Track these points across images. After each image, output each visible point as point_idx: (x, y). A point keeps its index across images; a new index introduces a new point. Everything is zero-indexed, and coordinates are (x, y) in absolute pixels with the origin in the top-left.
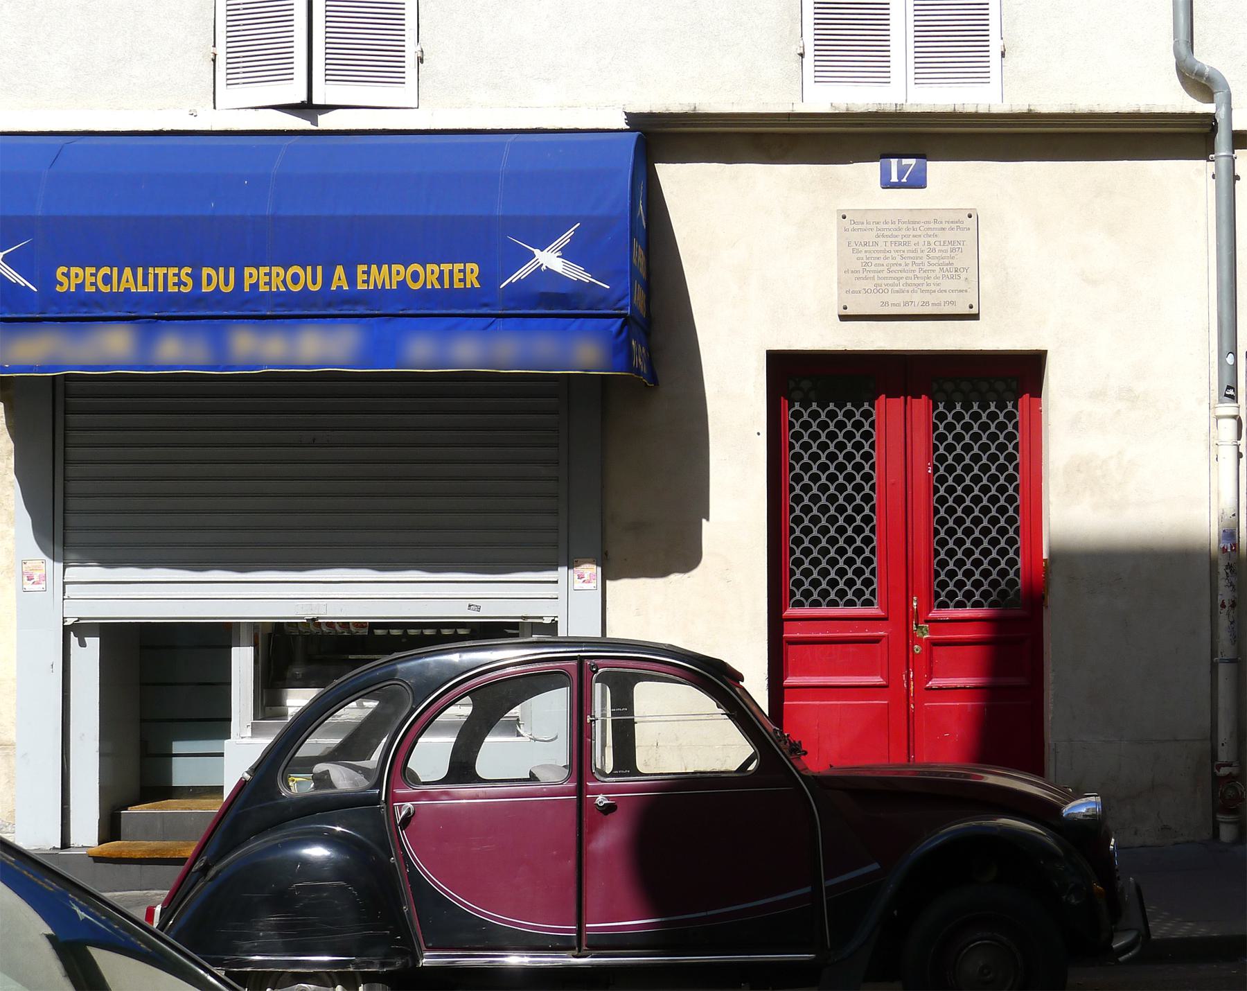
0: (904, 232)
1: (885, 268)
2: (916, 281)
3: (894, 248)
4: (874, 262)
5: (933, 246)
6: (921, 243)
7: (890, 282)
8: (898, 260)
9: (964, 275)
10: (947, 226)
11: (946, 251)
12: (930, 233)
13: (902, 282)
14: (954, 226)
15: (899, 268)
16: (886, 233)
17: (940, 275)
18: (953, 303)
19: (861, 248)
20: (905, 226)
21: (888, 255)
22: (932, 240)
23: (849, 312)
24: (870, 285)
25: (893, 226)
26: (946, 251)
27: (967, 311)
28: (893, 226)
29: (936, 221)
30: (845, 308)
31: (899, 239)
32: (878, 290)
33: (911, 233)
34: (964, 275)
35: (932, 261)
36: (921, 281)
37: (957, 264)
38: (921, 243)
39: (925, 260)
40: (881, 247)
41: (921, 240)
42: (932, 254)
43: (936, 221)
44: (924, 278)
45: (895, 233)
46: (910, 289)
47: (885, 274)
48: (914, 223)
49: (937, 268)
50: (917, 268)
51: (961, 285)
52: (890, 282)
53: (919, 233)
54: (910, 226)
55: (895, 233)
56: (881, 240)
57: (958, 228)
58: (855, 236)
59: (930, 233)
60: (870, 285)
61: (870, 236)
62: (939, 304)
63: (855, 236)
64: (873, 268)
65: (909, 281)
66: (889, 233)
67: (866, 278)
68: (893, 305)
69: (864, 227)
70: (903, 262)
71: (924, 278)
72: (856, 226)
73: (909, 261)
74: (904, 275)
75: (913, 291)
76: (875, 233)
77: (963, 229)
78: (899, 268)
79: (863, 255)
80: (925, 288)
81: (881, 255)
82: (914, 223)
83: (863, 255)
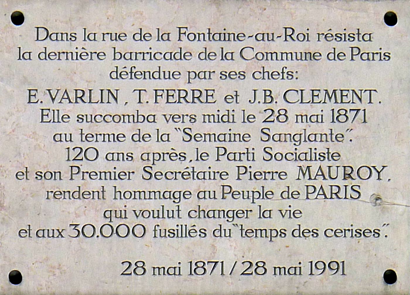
0: (194, 64)
1: (138, 165)
2: (230, 204)
3: (164, 108)
4: (104, 148)
5: (281, 104)
6: (245, 96)
7: (153, 205)
8: (177, 142)
9: (369, 188)
10: (323, 47)
11: (319, 119)
12: (274, 66)
13: (186, 205)
14: (344, 46)
15: (177, 166)
16: (141, 65)
17: (300, 186)
19: (66, 108)
20: (197, 47)
21: (146, 128)
22: (278, 87)
24: (91, 214)
25: (164, 47)
26: (319, 119)
28: (164, 47)
29: (289, 34)
31: (181, 84)
32: (114, 227)
33: (217, 65)
34: (369, 188)
35: (277, 148)
36: (240, 204)
37: (352, 155)
38: (245, 96)
39: (256, 143)
40: (128, 104)
41: (245, 87)
42: (276, 128)
43: (289, 34)
44: (252, 196)
45: (169, 66)
46: (211, 225)
47: (136, 183)
48: (225, 37)
49: (292, 168)
50: (231, 167)
51: (364, 215)
52: (153, 205)
53: (238, 65)
54: (215, 46)
55: (169, 66)
56: (126, 87)
57: (357, 53)
58: (51, 74)
59: (274, 66)
60: (91, 214)
61: (94, 75)
62: (297, 271)
63: (51, 74)
64: (101, 165)
65: (207, 204)
66: (151, 66)
67: (82, 195)
68: (159, 270)
69: (79, 44)
71: (252, 196)
72: (52, 47)
74: (193, 185)
75: (219, 233)
76: (108, 65)
77: (370, 57)
78: (177, 166)
79: (71, 127)
80: (253, 222)
81: (126, 129)
82: (225, 37)
83: (71, 127)
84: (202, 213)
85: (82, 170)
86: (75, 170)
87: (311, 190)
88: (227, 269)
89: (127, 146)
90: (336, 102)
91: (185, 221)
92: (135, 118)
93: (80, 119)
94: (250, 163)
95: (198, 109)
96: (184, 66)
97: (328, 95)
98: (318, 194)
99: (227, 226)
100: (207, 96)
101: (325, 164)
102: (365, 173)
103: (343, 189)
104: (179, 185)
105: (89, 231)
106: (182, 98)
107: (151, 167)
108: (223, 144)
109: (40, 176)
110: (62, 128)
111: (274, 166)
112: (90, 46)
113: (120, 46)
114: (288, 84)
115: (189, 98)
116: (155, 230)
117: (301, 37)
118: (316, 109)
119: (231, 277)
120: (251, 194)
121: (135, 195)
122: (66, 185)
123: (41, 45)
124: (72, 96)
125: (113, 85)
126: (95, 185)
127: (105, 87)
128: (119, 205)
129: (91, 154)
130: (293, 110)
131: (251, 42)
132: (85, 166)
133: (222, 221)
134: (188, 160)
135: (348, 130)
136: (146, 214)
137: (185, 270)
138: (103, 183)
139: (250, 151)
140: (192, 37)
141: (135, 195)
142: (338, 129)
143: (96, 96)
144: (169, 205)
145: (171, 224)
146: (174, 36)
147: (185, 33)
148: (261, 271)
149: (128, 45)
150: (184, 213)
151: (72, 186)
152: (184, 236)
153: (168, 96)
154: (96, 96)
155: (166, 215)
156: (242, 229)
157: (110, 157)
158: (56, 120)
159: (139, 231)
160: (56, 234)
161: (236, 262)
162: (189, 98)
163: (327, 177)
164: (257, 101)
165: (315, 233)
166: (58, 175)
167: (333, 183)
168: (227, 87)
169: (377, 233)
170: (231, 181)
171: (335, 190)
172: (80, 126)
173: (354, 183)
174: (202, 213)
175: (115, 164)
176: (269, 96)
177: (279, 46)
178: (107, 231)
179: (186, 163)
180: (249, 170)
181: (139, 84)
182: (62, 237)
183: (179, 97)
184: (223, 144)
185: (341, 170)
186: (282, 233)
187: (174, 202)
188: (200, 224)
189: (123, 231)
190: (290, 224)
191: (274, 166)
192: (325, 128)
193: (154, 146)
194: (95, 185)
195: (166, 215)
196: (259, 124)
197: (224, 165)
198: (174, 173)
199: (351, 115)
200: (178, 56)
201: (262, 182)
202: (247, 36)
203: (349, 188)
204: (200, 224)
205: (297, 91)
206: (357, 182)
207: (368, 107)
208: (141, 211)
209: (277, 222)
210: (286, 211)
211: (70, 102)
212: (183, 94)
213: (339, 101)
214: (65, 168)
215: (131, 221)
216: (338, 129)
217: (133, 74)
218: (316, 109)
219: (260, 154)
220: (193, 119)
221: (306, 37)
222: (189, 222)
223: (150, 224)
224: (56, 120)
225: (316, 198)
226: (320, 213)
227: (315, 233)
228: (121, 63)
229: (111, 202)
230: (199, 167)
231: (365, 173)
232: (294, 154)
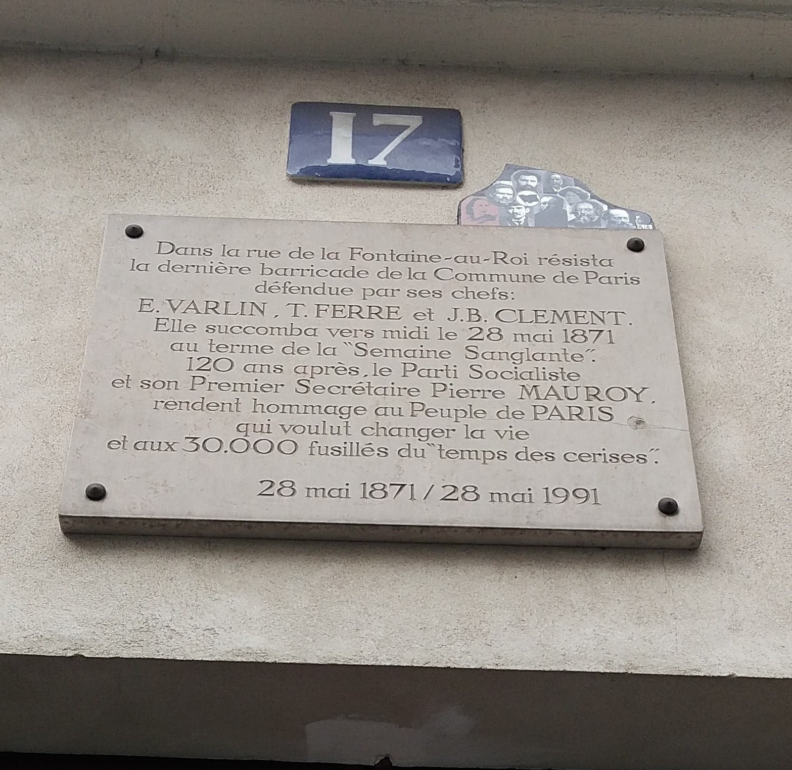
1: (289, 378)
2: (421, 422)
4: (241, 360)
8: (347, 356)
9: (625, 410)
10: (546, 270)
14: (578, 271)
15: (346, 380)
16: (297, 281)
18: (587, 495)
19: (191, 318)
20: (374, 267)
22: (487, 307)
23: (114, 507)
24: (220, 427)
27: (653, 522)
28: (329, 265)
30: (96, 494)
31: (355, 299)
32: (249, 440)
34: (625, 410)
41: (442, 308)
45: (342, 283)
46: (394, 444)
47: (287, 395)
49: (512, 388)
50: (426, 385)
51: (623, 439)
53: (432, 284)
56: (277, 303)
60: (220, 427)
64: (237, 375)
66: (316, 282)
68: (313, 491)
69: (216, 259)
70: (366, 364)
73: (396, 363)
78: (346, 380)
80: (458, 442)
81: (277, 341)
84: (381, 431)
85: (208, 380)
86: (199, 380)
87: (540, 410)
88: (420, 493)
89: (274, 358)
90: (569, 323)
91: (356, 437)
92: (289, 331)
93: (210, 329)
94: (452, 380)
95: (374, 324)
96: (358, 283)
97: (558, 316)
98: (551, 415)
99: (417, 445)
100: (389, 312)
101: (559, 385)
102: (617, 394)
103: (587, 411)
104: (350, 400)
105: (212, 445)
106: (354, 312)
107: (309, 381)
108: (413, 360)
109: (146, 384)
110: (184, 338)
111: (484, 384)
112: (229, 262)
113: (269, 262)
114: (500, 304)
115: (364, 313)
116: (312, 447)
117: (517, 261)
118: (544, 329)
119: (425, 503)
120: (453, 412)
121: (281, 409)
122: (183, 394)
123: (163, 259)
124: (201, 307)
125: (259, 299)
126: (228, 396)
127: (248, 300)
128: (261, 418)
129: (223, 365)
130: (508, 331)
131: (451, 264)
132: (211, 377)
133: (412, 440)
134: (362, 374)
135: (588, 350)
136: (299, 430)
137: (356, 492)
138: (238, 394)
139: (451, 367)
140: (369, 257)
141: (281, 409)
142: (572, 349)
143: (235, 308)
144: (333, 420)
145: (337, 441)
146: (345, 255)
147: (359, 253)
148: (470, 496)
149: (283, 261)
150: (355, 430)
151: (194, 397)
152: (355, 453)
153: (335, 311)
154: (235, 308)
155: (328, 431)
156: (440, 450)
157: (249, 368)
158: (176, 329)
159: (287, 447)
160: (164, 446)
161: (433, 485)
162: (364, 313)
163: (562, 396)
164: (459, 319)
165: (550, 457)
166: (173, 385)
167: (571, 403)
168: (422, 305)
169: (642, 459)
170: (425, 397)
171: (576, 411)
172: (210, 336)
173: (601, 404)
174: (381, 431)
175: (258, 375)
176: (475, 315)
177: (486, 268)
178: (240, 446)
179: (359, 377)
180: (449, 387)
181: (296, 298)
182: (172, 450)
183: (351, 313)
184: (413, 360)
185: (582, 392)
186: (502, 455)
187: (341, 417)
188: (378, 442)
189: (263, 447)
190: (511, 447)
191: (484, 384)
192: (557, 346)
193: (312, 359)
194: (228, 396)
195: (328, 431)
196: (463, 340)
197: (413, 380)
198: (342, 388)
199: (592, 336)
200: (349, 274)
201: (470, 401)
202: (443, 258)
203: (596, 411)
204: (378, 442)
205: (514, 311)
206: (607, 402)
207: (614, 329)
208: (291, 426)
209: (492, 443)
210: (506, 431)
211: (198, 312)
212: (355, 310)
213: (573, 321)
214: (185, 379)
215: (277, 436)
216: (572, 349)
217: (287, 289)
218: (544, 329)
219: (464, 370)
220: (369, 334)
221: (523, 261)
222: (363, 441)
223: (305, 441)
224: (176, 329)
225: (549, 419)
226: (551, 434)
227: (550, 457)
228: (271, 280)
229: (246, 414)
230: (376, 382)
231: (617, 394)
232: (514, 373)
